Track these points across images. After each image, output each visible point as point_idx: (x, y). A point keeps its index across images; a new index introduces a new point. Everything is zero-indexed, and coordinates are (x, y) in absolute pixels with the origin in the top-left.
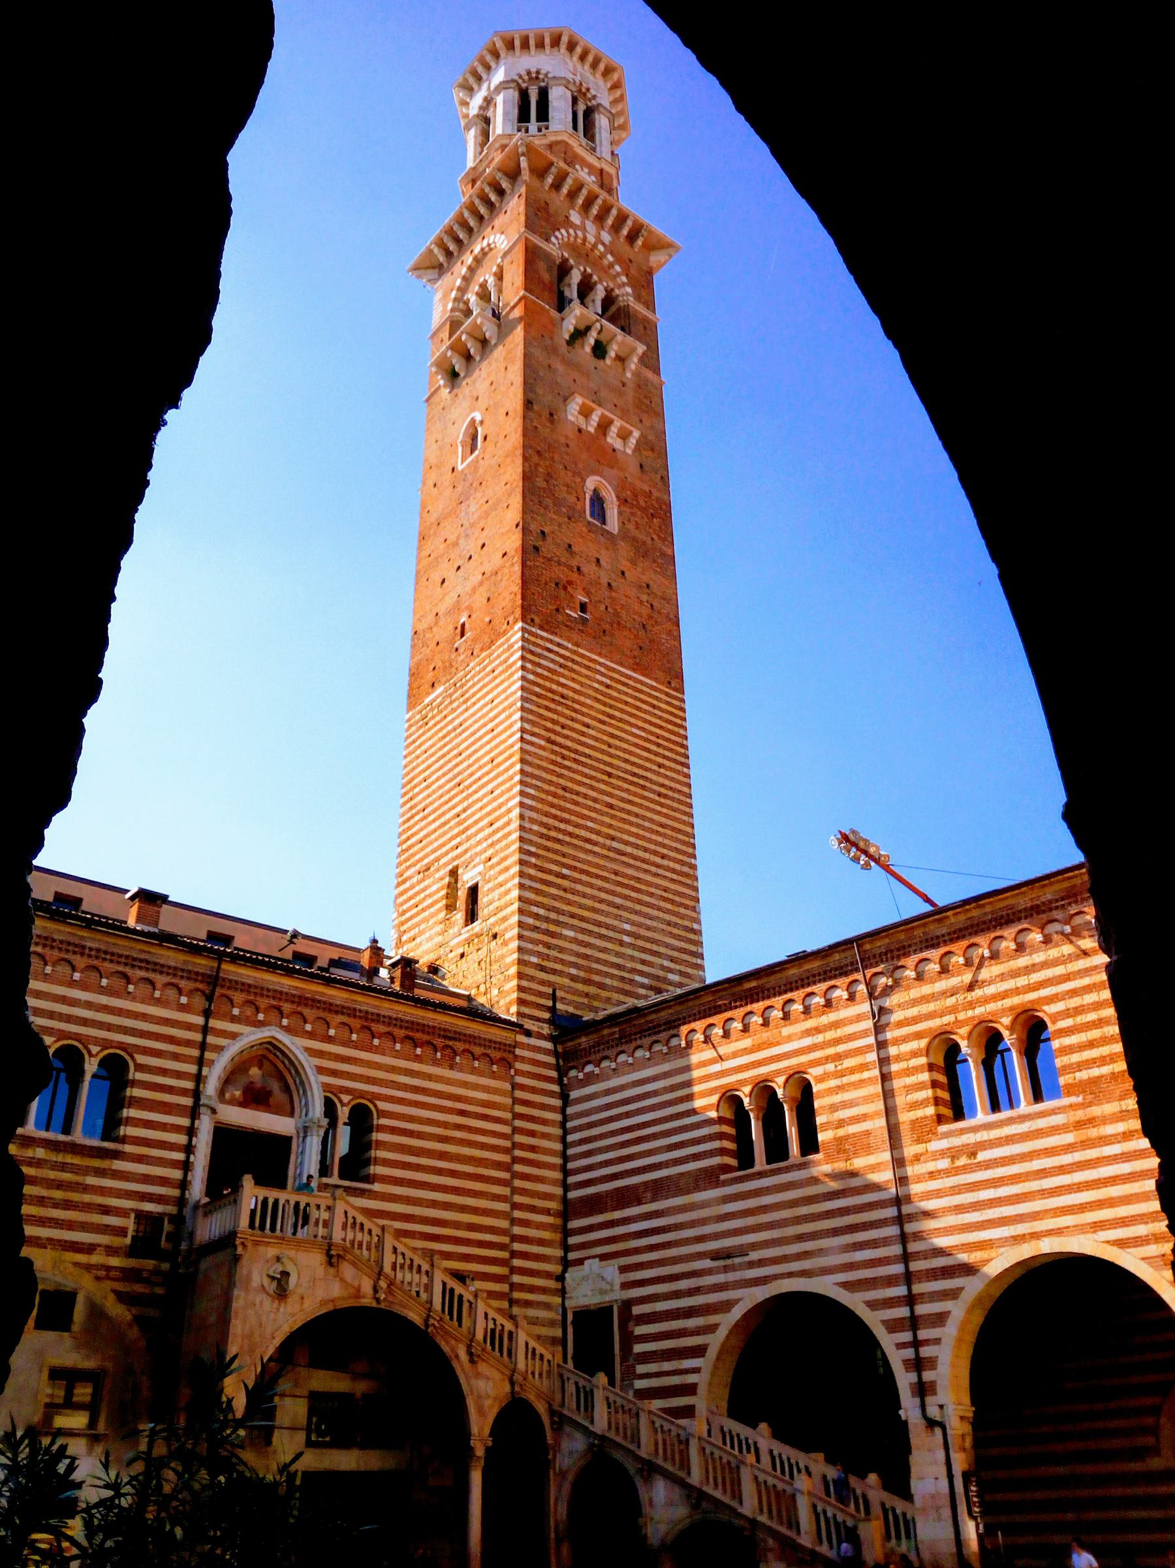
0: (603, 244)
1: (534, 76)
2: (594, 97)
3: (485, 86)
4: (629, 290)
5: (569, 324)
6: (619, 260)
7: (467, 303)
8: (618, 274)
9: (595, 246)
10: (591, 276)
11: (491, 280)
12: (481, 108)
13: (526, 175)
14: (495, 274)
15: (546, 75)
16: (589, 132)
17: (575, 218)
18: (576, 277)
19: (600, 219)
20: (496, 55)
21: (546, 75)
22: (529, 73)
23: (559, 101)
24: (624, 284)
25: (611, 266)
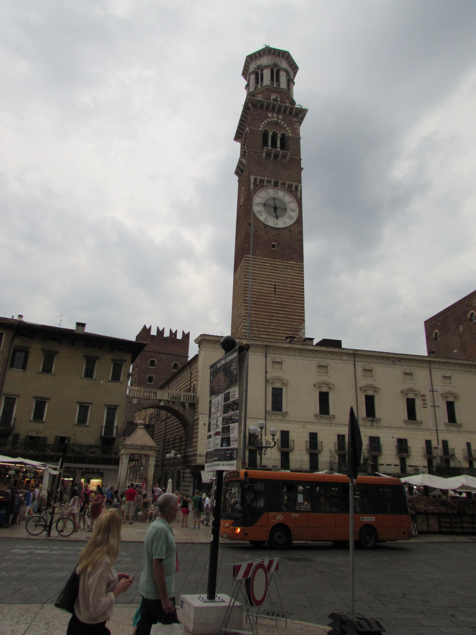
0: (280, 119)
1: (259, 67)
2: (279, 66)
4: (289, 131)
5: (264, 155)
6: (285, 123)
8: (285, 128)
9: (277, 121)
10: (276, 132)
13: (252, 108)
16: (278, 80)
17: (270, 115)
18: (270, 133)
19: (279, 112)
20: (249, 64)
25: (283, 125)
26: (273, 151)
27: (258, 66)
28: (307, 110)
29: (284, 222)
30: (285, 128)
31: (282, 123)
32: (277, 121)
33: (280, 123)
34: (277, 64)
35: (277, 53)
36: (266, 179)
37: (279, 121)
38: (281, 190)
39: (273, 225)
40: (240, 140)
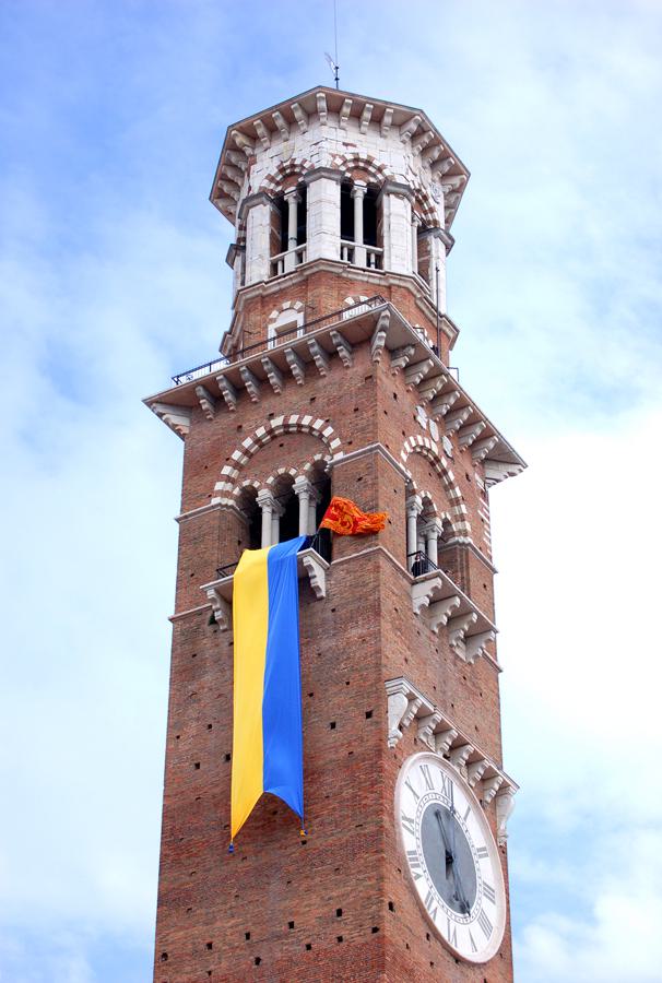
1: (362, 166)
3: (278, 147)
7: (249, 497)
11: (301, 483)
12: (271, 179)
15: (380, 170)
17: (422, 417)
20: (311, 114)
21: (380, 170)
22: (356, 160)
23: (398, 216)
24: (462, 518)
26: (457, 601)
27: (356, 160)
28: (525, 466)
29: (472, 939)
30: (455, 502)
31: (451, 476)
32: (437, 460)
33: (445, 472)
36: (439, 717)
37: (444, 462)
38: (463, 785)
39: (445, 935)
40: (182, 422)
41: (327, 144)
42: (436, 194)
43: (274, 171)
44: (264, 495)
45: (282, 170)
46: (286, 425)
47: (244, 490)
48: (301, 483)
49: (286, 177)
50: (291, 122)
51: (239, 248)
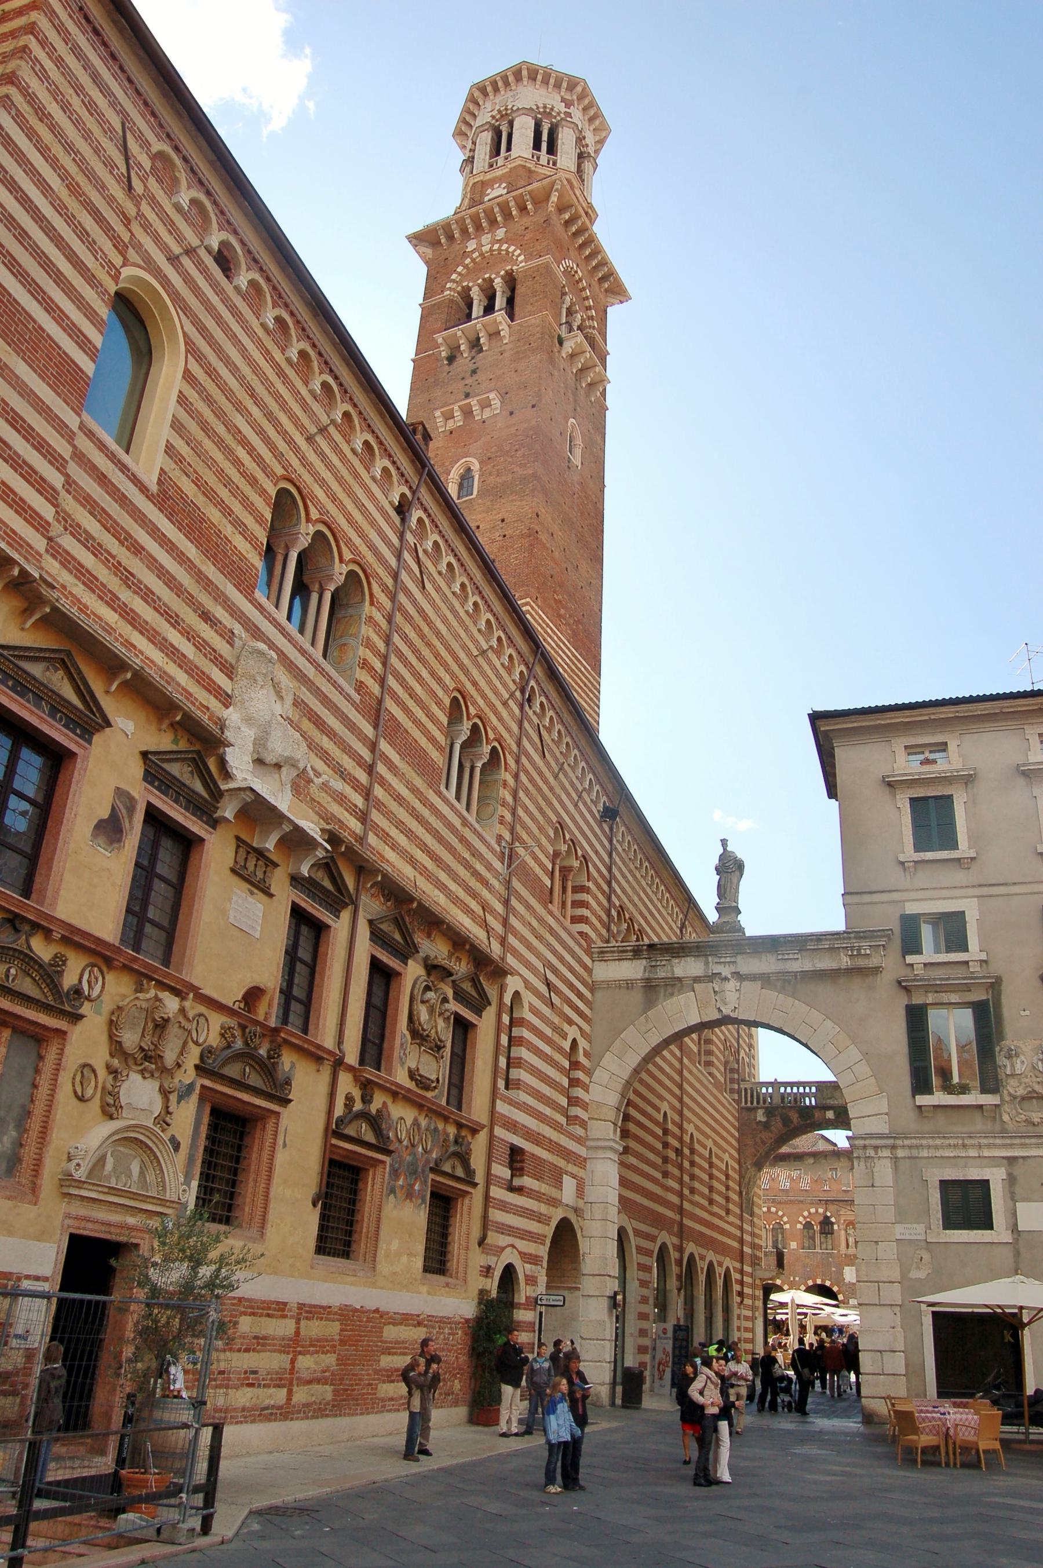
1: (548, 113)
2: (587, 145)
3: (499, 99)
12: (493, 117)
14: (502, 277)
22: (545, 107)
24: (592, 318)
34: (584, 138)
35: (592, 112)
40: (429, 252)
41: (530, 96)
42: (590, 139)
43: (495, 113)
44: (475, 293)
45: (499, 111)
46: (491, 250)
47: (463, 287)
48: (498, 283)
49: (502, 116)
50: (507, 84)
51: (470, 161)
